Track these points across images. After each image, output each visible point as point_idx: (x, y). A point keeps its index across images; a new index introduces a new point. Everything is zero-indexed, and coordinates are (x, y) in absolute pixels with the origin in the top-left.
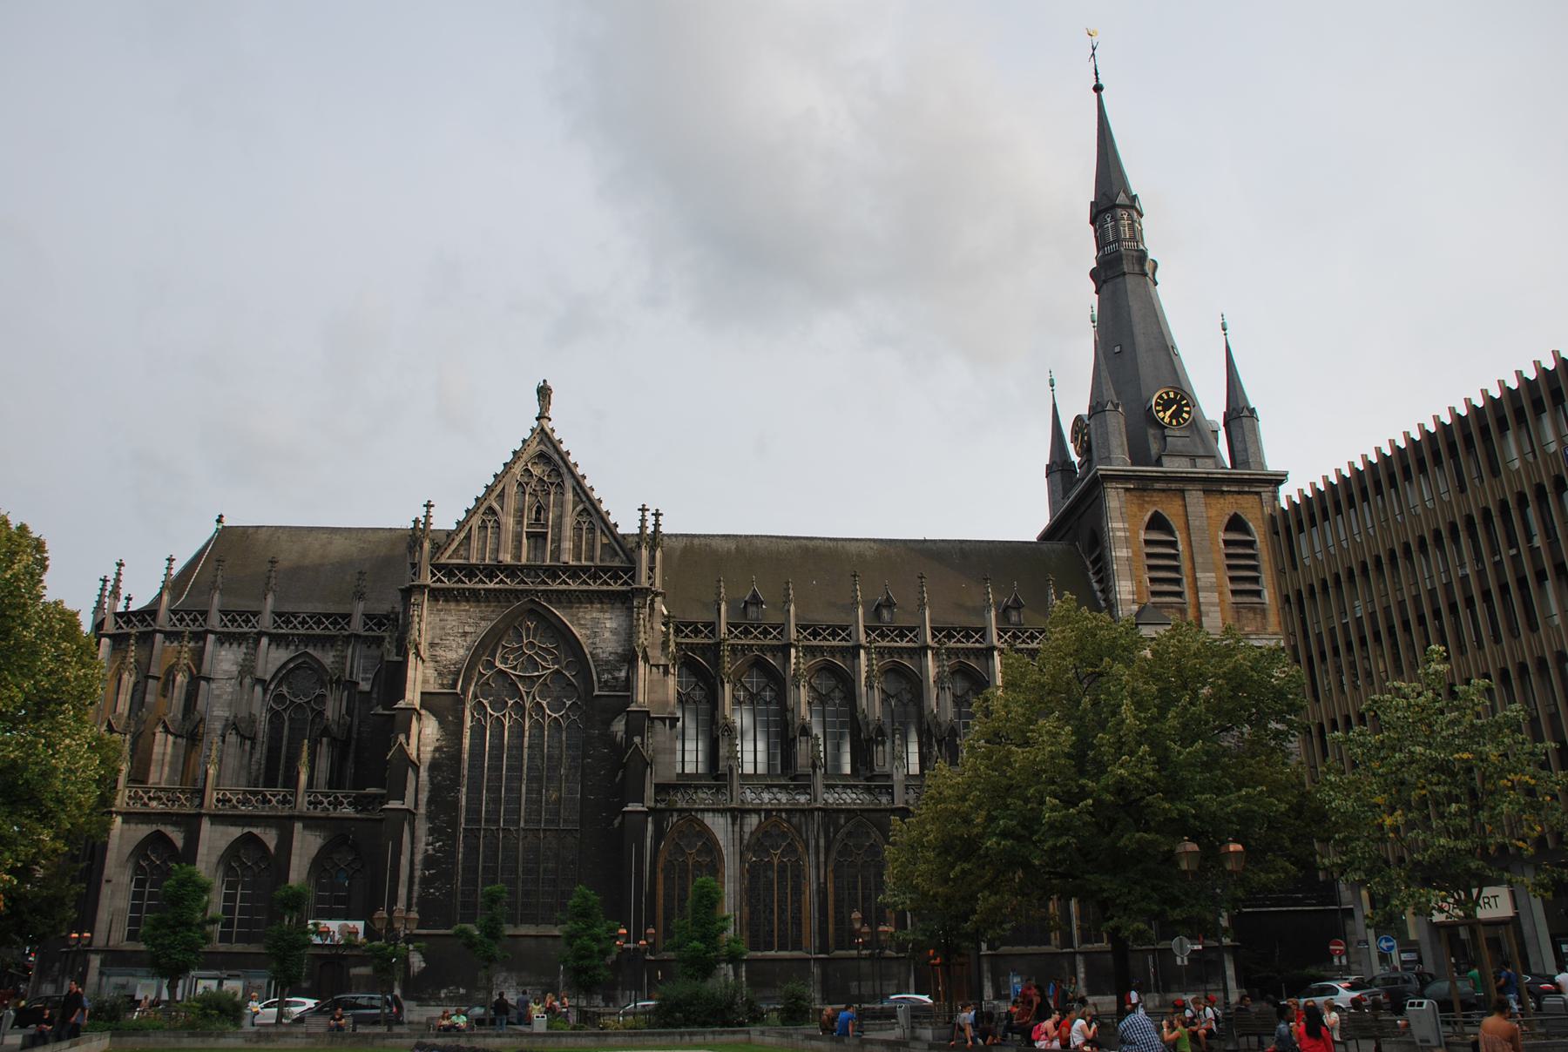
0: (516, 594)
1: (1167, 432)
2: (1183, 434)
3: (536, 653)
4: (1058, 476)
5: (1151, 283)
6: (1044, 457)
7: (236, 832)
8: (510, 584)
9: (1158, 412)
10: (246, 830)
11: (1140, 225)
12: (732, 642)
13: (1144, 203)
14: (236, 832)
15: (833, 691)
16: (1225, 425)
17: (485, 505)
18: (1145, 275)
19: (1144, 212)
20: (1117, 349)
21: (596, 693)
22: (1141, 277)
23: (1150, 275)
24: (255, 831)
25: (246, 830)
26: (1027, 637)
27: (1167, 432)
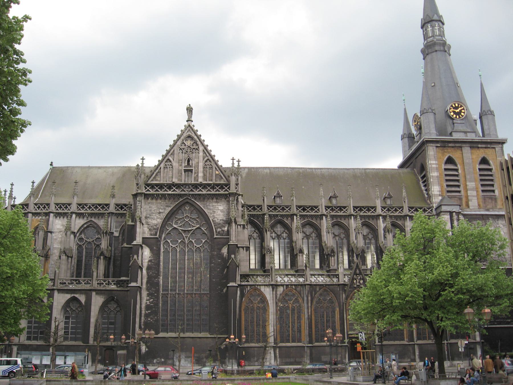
0: (180, 196)
1: (454, 121)
2: (462, 122)
4: (406, 140)
5: (448, 55)
8: (178, 192)
11: (443, 29)
12: (270, 213)
13: (445, 20)
16: (481, 118)
17: (166, 158)
18: (446, 51)
19: (445, 23)
20: (433, 84)
21: (215, 236)
22: (443, 53)
23: (447, 51)
26: (394, 210)
27: (454, 121)
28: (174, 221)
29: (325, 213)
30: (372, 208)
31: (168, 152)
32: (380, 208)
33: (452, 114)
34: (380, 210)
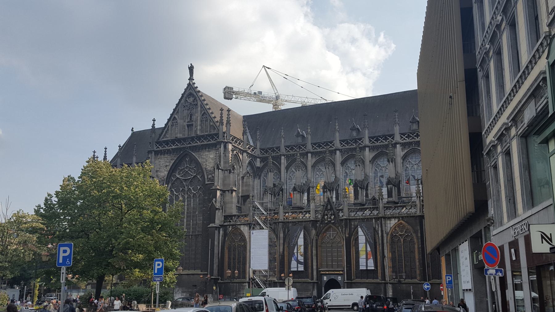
0: (180, 149)
3: (189, 170)
8: (180, 146)
12: (330, 149)
17: (173, 117)
21: (206, 183)
26: (415, 136)
28: (177, 172)
29: (340, 147)
30: (390, 136)
31: (174, 110)
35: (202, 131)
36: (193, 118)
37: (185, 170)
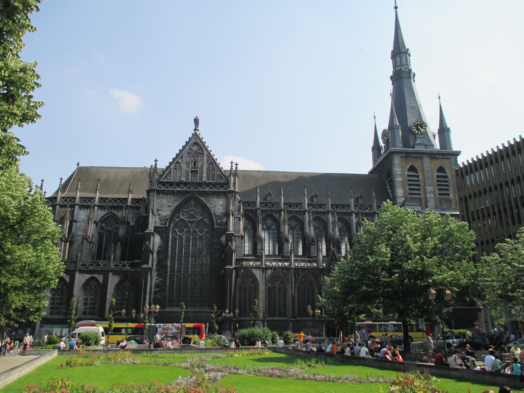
0: (186, 192)
1: (417, 136)
3: (194, 213)
4: (376, 151)
6: (372, 144)
7: (88, 276)
8: (185, 189)
9: (414, 129)
10: (92, 275)
11: (409, 59)
12: (261, 209)
13: (411, 52)
14: (88, 276)
15: (296, 226)
17: (176, 161)
19: (411, 55)
20: (399, 106)
21: (215, 227)
24: (95, 276)
25: (92, 275)
26: (365, 208)
27: (417, 136)
28: (181, 213)
31: (177, 155)
32: (376, 207)
33: (415, 130)
34: (376, 209)
35: (208, 179)
36: (198, 166)
37: (190, 213)
